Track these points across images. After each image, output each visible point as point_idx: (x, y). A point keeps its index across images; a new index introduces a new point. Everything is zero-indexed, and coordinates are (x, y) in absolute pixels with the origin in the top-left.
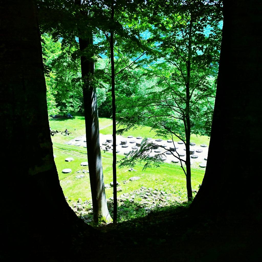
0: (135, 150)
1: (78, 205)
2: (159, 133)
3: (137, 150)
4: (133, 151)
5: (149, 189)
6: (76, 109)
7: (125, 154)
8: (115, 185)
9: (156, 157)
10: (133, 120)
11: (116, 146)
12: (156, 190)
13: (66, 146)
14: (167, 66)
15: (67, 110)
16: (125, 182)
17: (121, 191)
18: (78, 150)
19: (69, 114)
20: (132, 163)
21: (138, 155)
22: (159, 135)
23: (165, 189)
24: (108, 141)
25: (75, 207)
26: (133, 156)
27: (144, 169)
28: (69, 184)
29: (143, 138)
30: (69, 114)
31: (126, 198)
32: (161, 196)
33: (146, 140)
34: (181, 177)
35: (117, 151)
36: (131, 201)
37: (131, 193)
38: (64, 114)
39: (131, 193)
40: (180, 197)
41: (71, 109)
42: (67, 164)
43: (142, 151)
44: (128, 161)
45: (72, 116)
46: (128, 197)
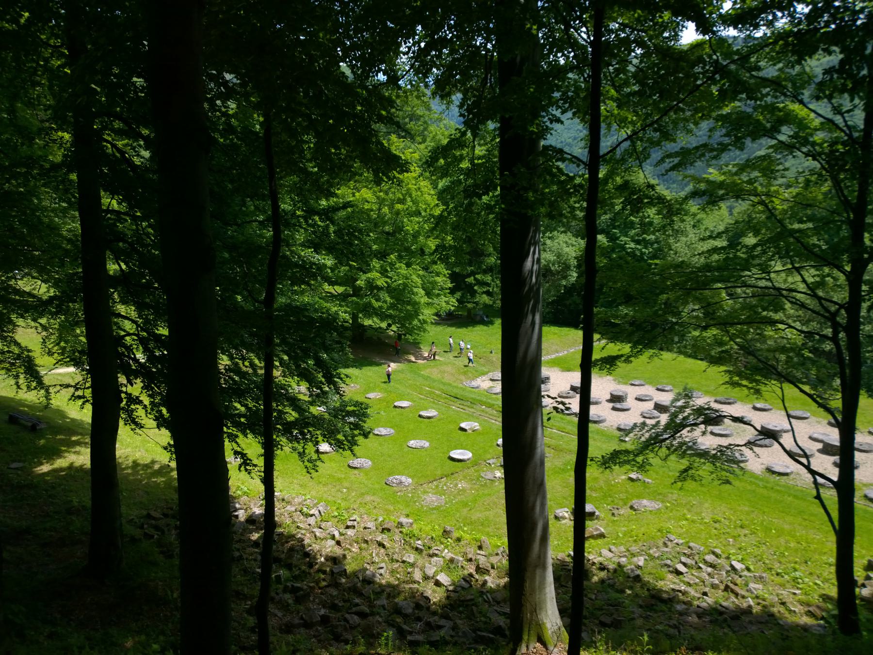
0: (650, 422)
1: (479, 557)
2: (736, 378)
3: (658, 422)
5: (692, 544)
7: (619, 429)
10: (651, 333)
12: (714, 553)
14: (781, 167)
16: (616, 512)
17: (602, 536)
18: (493, 405)
19: (481, 313)
20: (640, 459)
23: (746, 557)
24: (573, 388)
25: (471, 560)
26: (643, 439)
27: (679, 484)
28: (464, 490)
29: (680, 390)
30: (481, 313)
31: (616, 560)
32: (733, 575)
33: (688, 395)
36: (632, 570)
37: (635, 548)
38: (469, 311)
40: (797, 592)
41: (485, 299)
42: (462, 439)
43: (675, 427)
45: (487, 317)
46: (624, 559)
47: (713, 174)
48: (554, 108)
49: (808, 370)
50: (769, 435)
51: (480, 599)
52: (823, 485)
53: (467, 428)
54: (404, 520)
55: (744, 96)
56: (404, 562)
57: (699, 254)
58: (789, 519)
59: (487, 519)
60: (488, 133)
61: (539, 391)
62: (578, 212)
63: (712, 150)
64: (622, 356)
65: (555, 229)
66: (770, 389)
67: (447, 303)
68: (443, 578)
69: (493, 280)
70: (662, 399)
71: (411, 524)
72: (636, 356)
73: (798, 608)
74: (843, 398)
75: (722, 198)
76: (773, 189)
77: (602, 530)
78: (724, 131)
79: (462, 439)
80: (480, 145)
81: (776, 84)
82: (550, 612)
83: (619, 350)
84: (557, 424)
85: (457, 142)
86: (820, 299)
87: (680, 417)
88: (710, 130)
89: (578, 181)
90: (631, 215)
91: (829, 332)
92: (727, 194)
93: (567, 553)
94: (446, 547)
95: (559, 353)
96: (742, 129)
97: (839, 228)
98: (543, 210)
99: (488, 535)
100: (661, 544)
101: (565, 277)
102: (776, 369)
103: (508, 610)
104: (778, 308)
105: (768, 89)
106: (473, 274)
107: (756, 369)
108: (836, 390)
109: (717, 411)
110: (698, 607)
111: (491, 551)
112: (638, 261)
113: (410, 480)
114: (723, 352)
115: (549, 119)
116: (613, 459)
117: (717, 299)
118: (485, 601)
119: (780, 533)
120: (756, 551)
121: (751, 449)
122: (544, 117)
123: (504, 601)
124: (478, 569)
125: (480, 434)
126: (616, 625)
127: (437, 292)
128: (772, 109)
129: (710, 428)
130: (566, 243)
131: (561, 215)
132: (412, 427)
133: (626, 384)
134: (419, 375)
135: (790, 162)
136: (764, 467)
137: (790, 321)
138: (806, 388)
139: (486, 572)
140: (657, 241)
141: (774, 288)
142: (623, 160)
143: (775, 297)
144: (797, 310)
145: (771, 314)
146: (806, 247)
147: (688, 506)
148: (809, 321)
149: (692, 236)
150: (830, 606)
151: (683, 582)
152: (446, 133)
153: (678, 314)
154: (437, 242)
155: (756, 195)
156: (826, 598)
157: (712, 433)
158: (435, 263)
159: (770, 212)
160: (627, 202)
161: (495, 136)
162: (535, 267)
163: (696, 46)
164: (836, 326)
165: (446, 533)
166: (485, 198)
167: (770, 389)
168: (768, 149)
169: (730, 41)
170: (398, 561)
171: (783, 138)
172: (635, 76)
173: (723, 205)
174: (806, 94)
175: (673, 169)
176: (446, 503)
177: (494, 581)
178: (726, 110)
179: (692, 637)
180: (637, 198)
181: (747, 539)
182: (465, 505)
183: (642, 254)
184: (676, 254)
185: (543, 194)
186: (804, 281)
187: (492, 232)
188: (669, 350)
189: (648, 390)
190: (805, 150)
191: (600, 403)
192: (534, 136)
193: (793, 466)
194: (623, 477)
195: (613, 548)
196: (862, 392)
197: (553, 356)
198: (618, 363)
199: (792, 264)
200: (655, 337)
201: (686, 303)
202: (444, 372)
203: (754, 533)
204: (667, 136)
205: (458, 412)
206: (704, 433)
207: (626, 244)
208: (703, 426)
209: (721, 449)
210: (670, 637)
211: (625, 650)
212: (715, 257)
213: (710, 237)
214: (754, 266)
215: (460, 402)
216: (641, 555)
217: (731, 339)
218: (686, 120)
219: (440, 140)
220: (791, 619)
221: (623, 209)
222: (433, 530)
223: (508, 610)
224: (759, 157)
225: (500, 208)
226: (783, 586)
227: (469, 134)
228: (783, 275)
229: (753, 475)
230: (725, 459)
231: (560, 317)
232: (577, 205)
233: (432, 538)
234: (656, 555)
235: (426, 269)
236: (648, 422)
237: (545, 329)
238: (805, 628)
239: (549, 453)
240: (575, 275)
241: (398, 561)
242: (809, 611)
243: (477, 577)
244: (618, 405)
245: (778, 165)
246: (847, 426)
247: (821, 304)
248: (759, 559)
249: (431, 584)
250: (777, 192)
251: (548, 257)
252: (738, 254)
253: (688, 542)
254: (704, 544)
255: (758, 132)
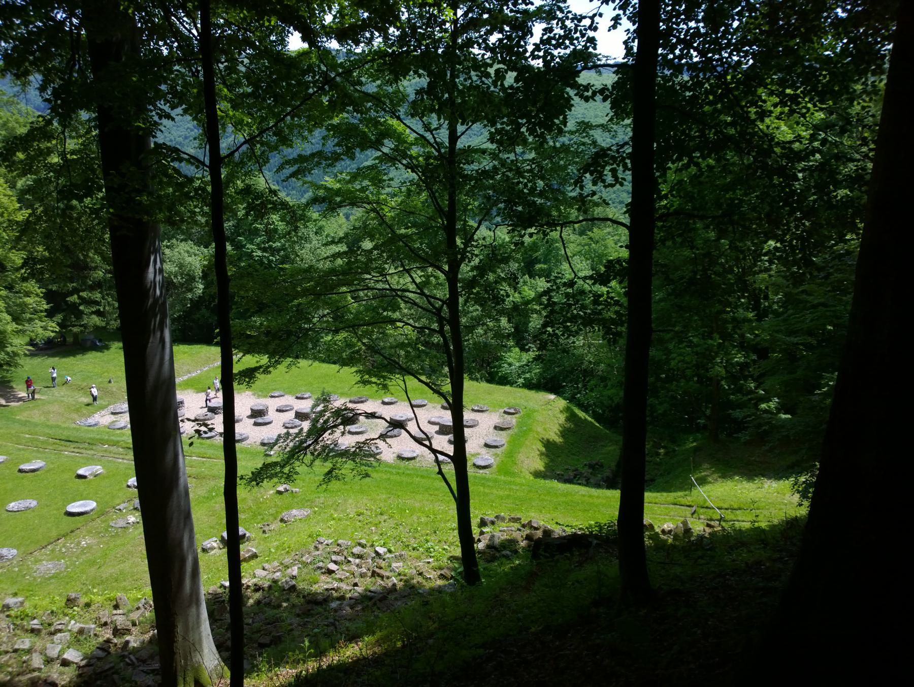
1: (115, 618)
4: (288, 434)
5: (340, 542)
6: (113, 322)
7: (263, 444)
8: (233, 542)
9: (359, 447)
10: (286, 344)
11: (236, 425)
12: (360, 544)
13: (77, 430)
15: (81, 326)
16: (266, 528)
17: (254, 556)
18: (118, 442)
20: (286, 470)
21: (305, 445)
22: (365, 383)
24: (213, 410)
25: (106, 624)
26: (288, 449)
27: (324, 486)
28: (89, 547)
30: (92, 337)
31: (270, 576)
32: (377, 560)
33: (325, 399)
34: (427, 500)
35: (237, 437)
36: (287, 582)
37: (288, 560)
38: (76, 336)
39: (286, 560)
40: (431, 560)
41: (96, 320)
42: (82, 487)
43: (317, 432)
44: (275, 464)
45: (100, 341)
46: (278, 574)
47: (329, 181)
48: (162, 102)
49: (423, 361)
50: (397, 425)
51: (122, 664)
52: (442, 462)
53: (87, 474)
54: (11, 601)
55: (351, 108)
56: (16, 651)
57: (325, 259)
58: (419, 497)
59: (122, 572)
60: (81, 124)
61: (176, 416)
62: (199, 218)
63: (326, 159)
64: (261, 367)
65: (173, 237)
66: (394, 383)
67: (45, 328)
68: (73, 655)
69: (103, 298)
70: (302, 407)
71: (22, 603)
72: (275, 367)
73: (432, 575)
74: (452, 383)
75: (340, 205)
76: (382, 197)
77: (254, 550)
78: (336, 140)
79: (82, 487)
80: (71, 137)
81: (376, 99)
82: (206, 651)
83: (257, 362)
84: (197, 451)
85: (39, 132)
86: (427, 296)
87: (321, 421)
88: (323, 138)
89: (197, 183)
90: (255, 221)
91: (435, 326)
92: (344, 201)
93: (219, 585)
94: (73, 618)
95: (194, 371)
96: (351, 140)
97: (436, 235)
98: (161, 216)
99: (125, 590)
100: (312, 548)
101: (190, 290)
102: (398, 364)
103: (156, 666)
104: (395, 308)
105: (370, 104)
106: (76, 291)
107: (381, 366)
108: (445, 376)
109: (353, 410)
110: (351, 598)
111: (130, 607)
112: (266, 268)
113: (14, 552)
114: (353, 353)
115: (157, 114)
116: (258, 477)
117: (344, 303)
118: (128, 664)
119: (413, 511)
120: (395, 533)
121: (384, 441)
122: (151, 111)
123: (152, 657)
124: (117, 632)
125: (104, 478)
126: (277, 641)
127: (28, 316)
128: (376, 123)
129: (348, 428)
130: (188, 252)
131: (182, 221)
132: (10, 485)
133: (265, 397)
134: (14, 421)
135: (393, 173)
136: (395, 455)
137: (405, 319)
138: (423, 378)
139: (127, 631)
140: (283, 248)
141: (391, 289)
142: (242, 163)
143: (391, 298)
144: (410, 309)
145: (390, 313)
146: (412, 250)
147: (334, 506)
148: (420, 318)
149: (315, 241)
150: (457, 566)
151: (335, 579)
152: (21, 120)
153: (309, 321)
154: (24, 254)
155: (368, 204)
156: (452, 558)
157: (350, 433)
158: (24, 279)
159: (381, 217)
160: (250, 208)
161: (90, 128)
162: (157, 279)
163: (303, 54)
164: (441, 321)
165: (70, 602)
166: (87, 200)
167: (394, 383)
168: (374, 159)
169: (334, 53)
170: (7, 652)
171: (386, 150)
172: (247, 76)
173: (342, 211)
174: (402, 111)
175: (293, 175)
176: (67, 568)
177: (134, 640)
178: (336, 121)
179: (348, 629)
180: (261, 204)
181: (386, 524)
182: (93, 563)
183: (270, 261)
184: (302, 260)
185: (159, 197)
186: (414, 281)
187: (99, 240)
188: (305, 358)
189: (289, 400)
190: (404, 162)
191: (241, 420)
192: (141, 133)
193: (419, 450)
194: (271, 492)
195: (267, 566)
196: (465, 375)
197: (185, 378)
198: (257, 375)
199: (403, 266)
200: (290, 346)
201: (318, 308)
202: (49, 412)
203: (392, 517)
204: (285, 141)
205: (72, 457)
206: (343, 434)
207: (253, 252)
208: (341, 427)
209: (359, 446)
210: (326, 635)
211: (288, 663)
212: (339, 261)
213: (333, 242)
214: (373, 269)
215: (73, 445)
216: (295, 565)
217: (360, 340)
218: (300, 126)
219: (13, 129)
220: (428, 585)
221: (247, 214)
222: (53, 602)
223: (156, 666)
224: (368, 167)
225: (108, 212)
226: (418, 558)
227: (55, 124)
228: (396, 277)
229: (388, 465)
230: (362, 454)
231: (192, 333)
232: (197, 210)
233: (52, 612)
234: (309, 561)
235: (10, 288)
236: (291, 431)
237: (175, 348)
238: (440, 590)
239: (192, 484)
240: (201, 286)
241: (7, 652)
242: (441, 575)
243: (115, 641)
244: (260, 420)
245: (385, 174)
246: (457, 408)
247: (430, 302)
248: (398, 539)
249: (57, 666)
250: (385, 200)
251: (169, 267)
252: (359, 257)
253: (336, 541)
254: (351, 538)
255: (366, 144)
